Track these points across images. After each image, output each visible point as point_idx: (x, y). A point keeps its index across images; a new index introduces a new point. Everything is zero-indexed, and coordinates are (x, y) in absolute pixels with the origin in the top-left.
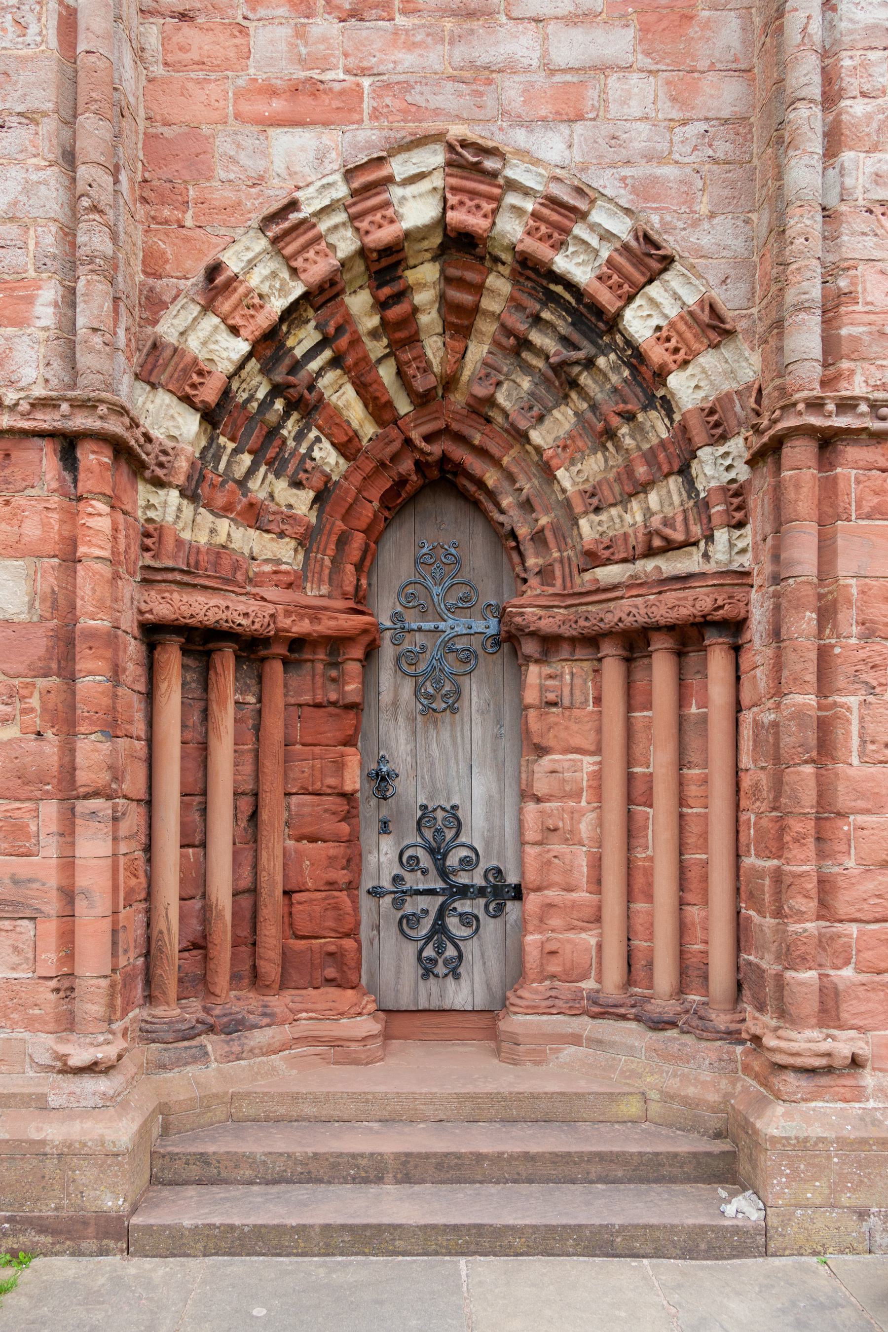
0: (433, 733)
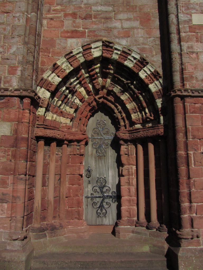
0: (100, 161)
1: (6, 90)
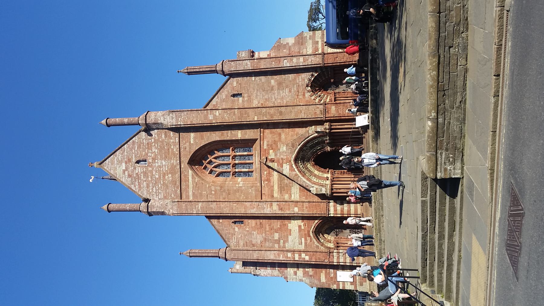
1: (323, 108)
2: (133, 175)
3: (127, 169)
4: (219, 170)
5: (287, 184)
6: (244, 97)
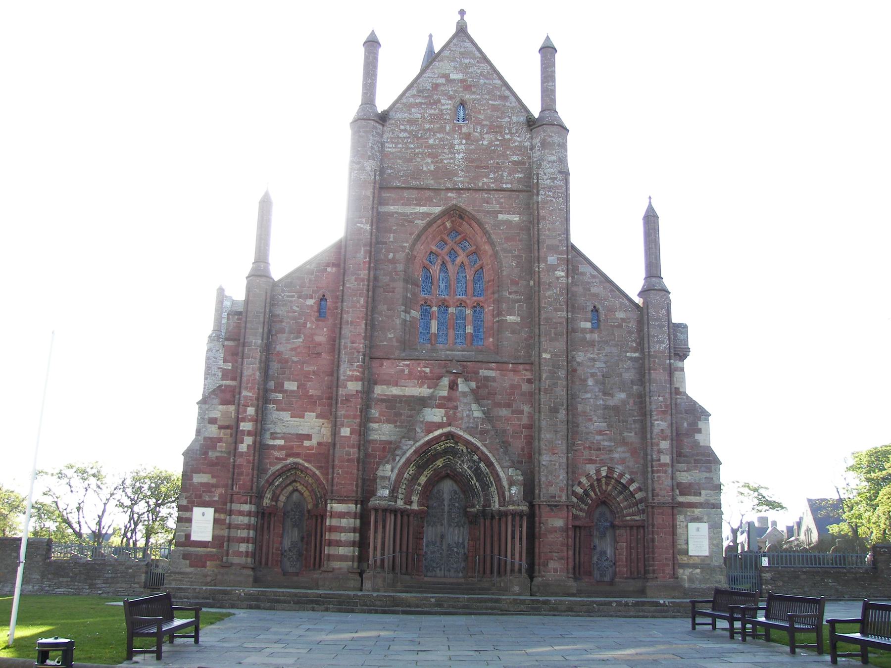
1: (560, 501)
2: (437, 94)
3: (449, 81)
4: (435, 269)
5: (401, 414)
6: (592, 331)
